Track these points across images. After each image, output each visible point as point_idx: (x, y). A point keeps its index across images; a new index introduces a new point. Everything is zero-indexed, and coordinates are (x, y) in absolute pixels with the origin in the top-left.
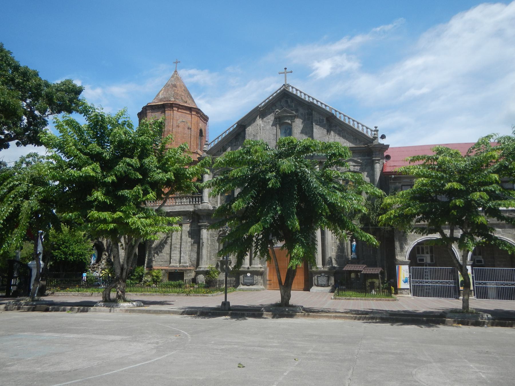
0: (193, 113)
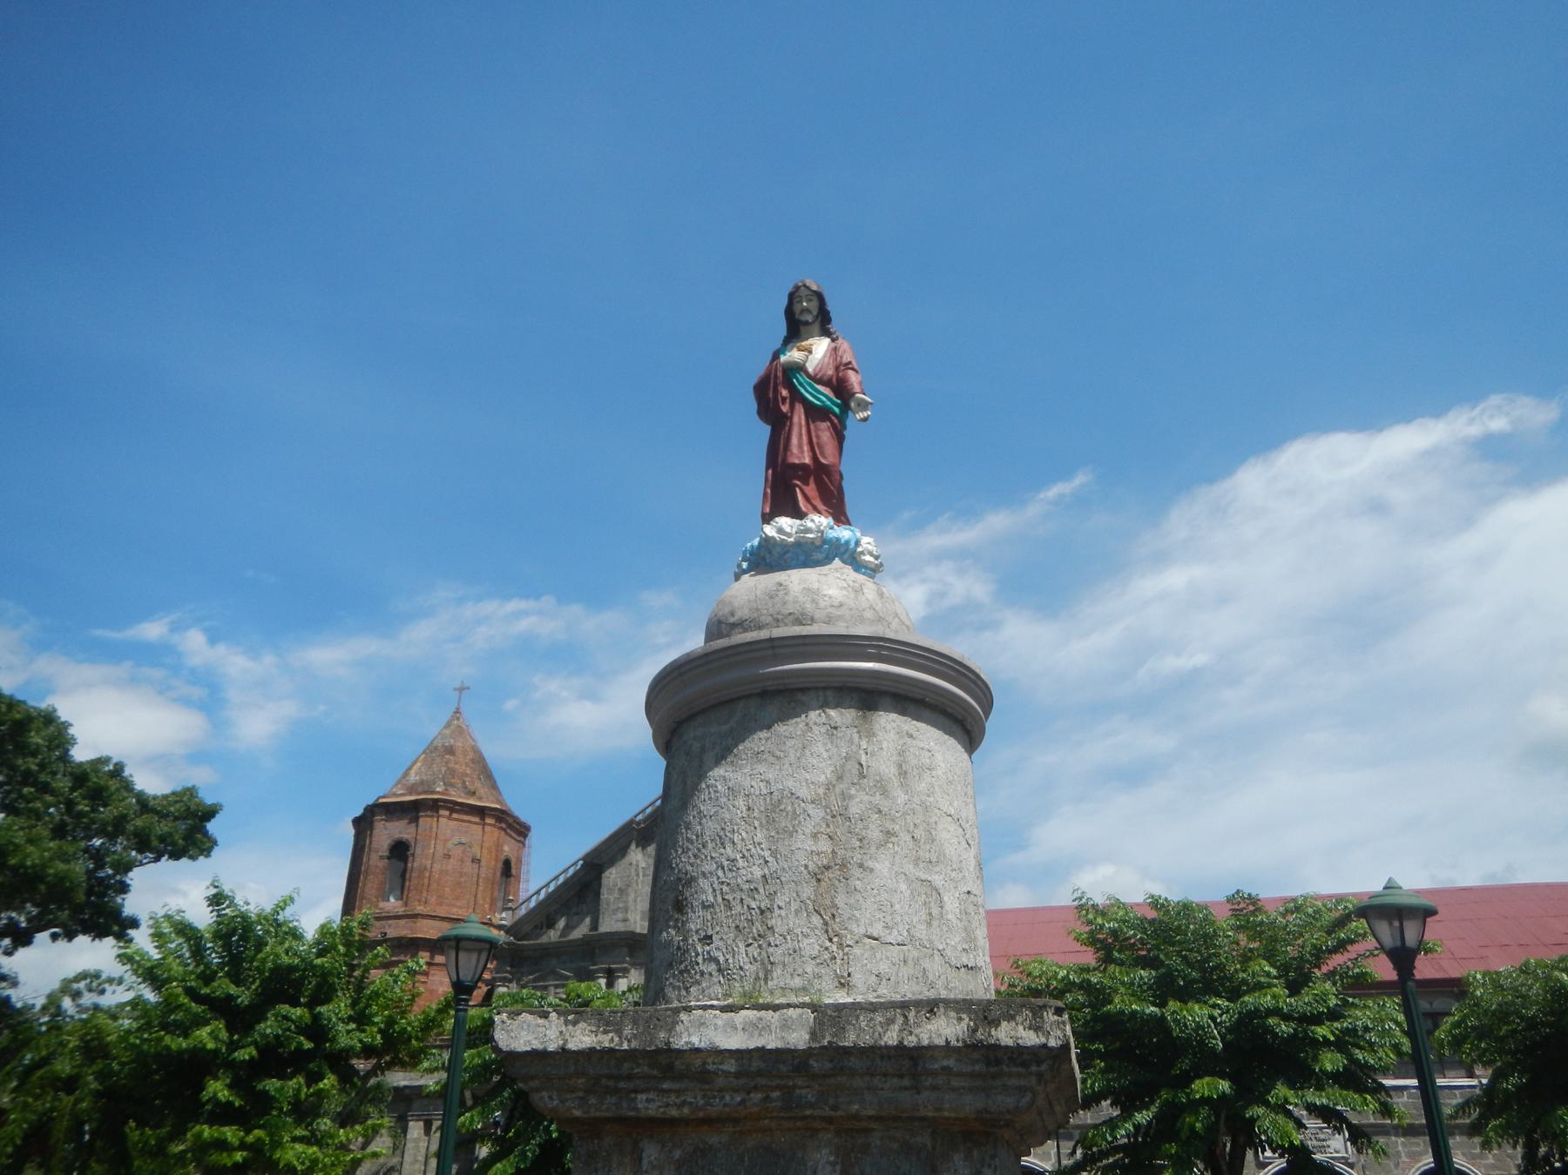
0: (488, 821)
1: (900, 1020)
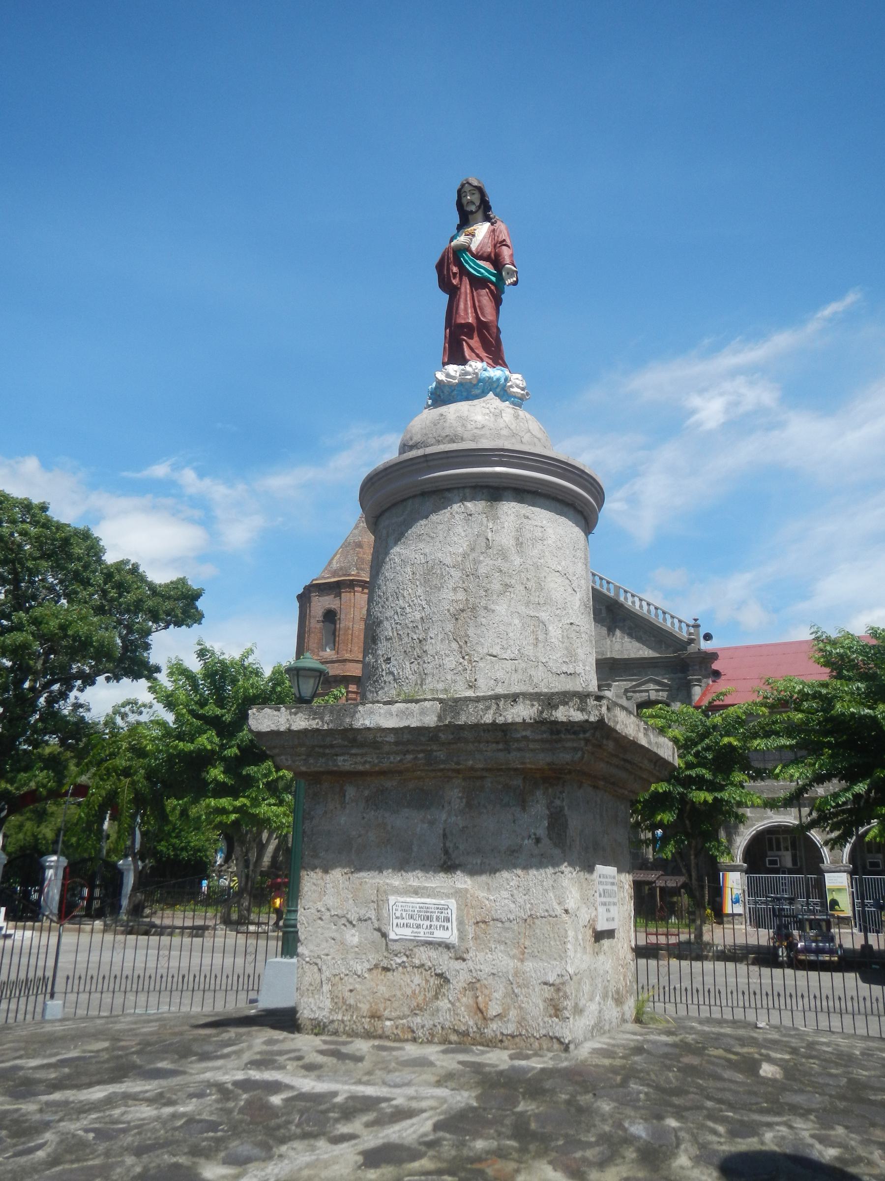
1: (494, 707)
